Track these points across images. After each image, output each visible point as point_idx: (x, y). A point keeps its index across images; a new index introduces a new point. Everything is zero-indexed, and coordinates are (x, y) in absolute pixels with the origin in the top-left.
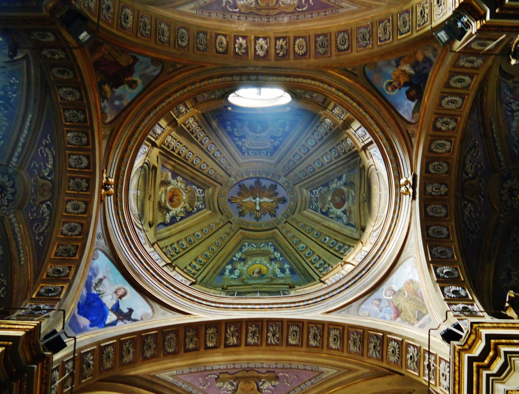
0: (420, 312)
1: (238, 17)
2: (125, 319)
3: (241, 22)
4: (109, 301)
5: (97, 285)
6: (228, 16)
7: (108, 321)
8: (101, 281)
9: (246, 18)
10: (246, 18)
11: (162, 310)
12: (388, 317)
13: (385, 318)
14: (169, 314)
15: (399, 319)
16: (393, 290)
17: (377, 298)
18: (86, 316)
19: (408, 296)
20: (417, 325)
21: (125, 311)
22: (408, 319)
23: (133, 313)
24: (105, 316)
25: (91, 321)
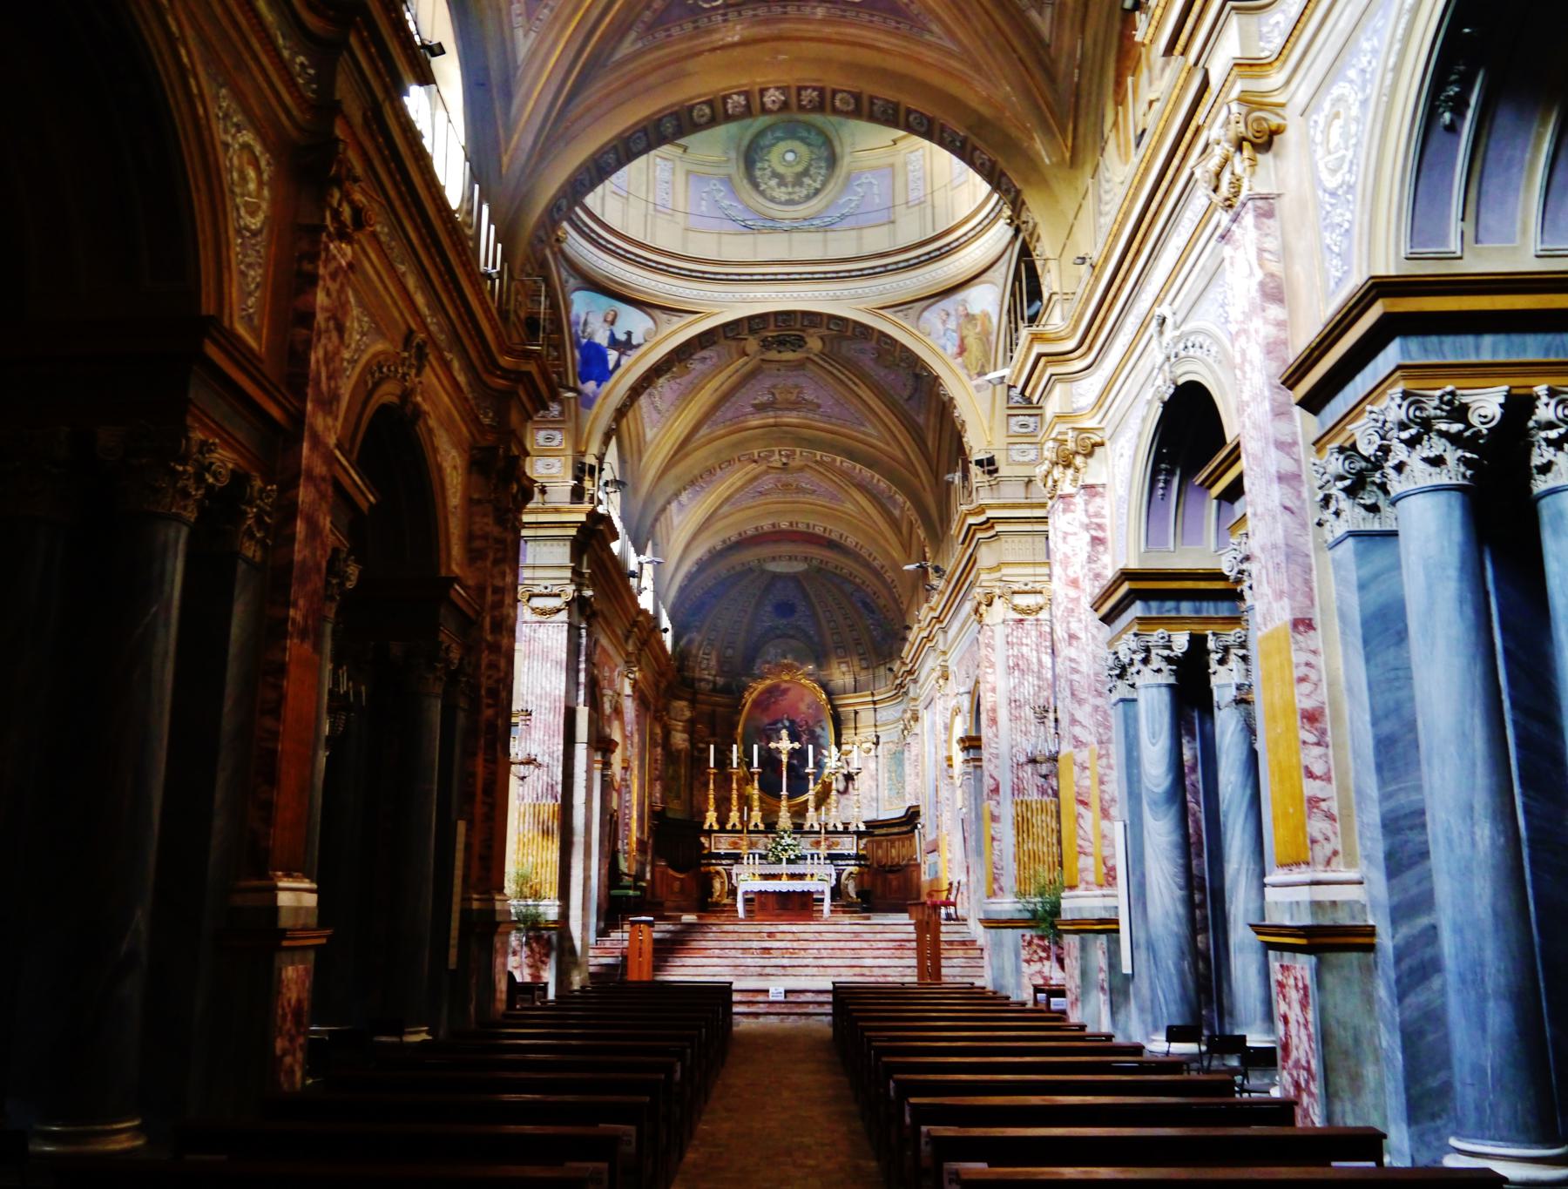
0: (983, 366)
1: (724, 15)
3: (730, 24)
4: (601, 338)
6: (703, 22)
9: (740, 14)
10: (740, 14)
11: (665, 317)
14: (675, 319)
15: (960, 360)
20: (975, 383)
21: (622, 337)
24: (606, 362)
25: (596, 380)
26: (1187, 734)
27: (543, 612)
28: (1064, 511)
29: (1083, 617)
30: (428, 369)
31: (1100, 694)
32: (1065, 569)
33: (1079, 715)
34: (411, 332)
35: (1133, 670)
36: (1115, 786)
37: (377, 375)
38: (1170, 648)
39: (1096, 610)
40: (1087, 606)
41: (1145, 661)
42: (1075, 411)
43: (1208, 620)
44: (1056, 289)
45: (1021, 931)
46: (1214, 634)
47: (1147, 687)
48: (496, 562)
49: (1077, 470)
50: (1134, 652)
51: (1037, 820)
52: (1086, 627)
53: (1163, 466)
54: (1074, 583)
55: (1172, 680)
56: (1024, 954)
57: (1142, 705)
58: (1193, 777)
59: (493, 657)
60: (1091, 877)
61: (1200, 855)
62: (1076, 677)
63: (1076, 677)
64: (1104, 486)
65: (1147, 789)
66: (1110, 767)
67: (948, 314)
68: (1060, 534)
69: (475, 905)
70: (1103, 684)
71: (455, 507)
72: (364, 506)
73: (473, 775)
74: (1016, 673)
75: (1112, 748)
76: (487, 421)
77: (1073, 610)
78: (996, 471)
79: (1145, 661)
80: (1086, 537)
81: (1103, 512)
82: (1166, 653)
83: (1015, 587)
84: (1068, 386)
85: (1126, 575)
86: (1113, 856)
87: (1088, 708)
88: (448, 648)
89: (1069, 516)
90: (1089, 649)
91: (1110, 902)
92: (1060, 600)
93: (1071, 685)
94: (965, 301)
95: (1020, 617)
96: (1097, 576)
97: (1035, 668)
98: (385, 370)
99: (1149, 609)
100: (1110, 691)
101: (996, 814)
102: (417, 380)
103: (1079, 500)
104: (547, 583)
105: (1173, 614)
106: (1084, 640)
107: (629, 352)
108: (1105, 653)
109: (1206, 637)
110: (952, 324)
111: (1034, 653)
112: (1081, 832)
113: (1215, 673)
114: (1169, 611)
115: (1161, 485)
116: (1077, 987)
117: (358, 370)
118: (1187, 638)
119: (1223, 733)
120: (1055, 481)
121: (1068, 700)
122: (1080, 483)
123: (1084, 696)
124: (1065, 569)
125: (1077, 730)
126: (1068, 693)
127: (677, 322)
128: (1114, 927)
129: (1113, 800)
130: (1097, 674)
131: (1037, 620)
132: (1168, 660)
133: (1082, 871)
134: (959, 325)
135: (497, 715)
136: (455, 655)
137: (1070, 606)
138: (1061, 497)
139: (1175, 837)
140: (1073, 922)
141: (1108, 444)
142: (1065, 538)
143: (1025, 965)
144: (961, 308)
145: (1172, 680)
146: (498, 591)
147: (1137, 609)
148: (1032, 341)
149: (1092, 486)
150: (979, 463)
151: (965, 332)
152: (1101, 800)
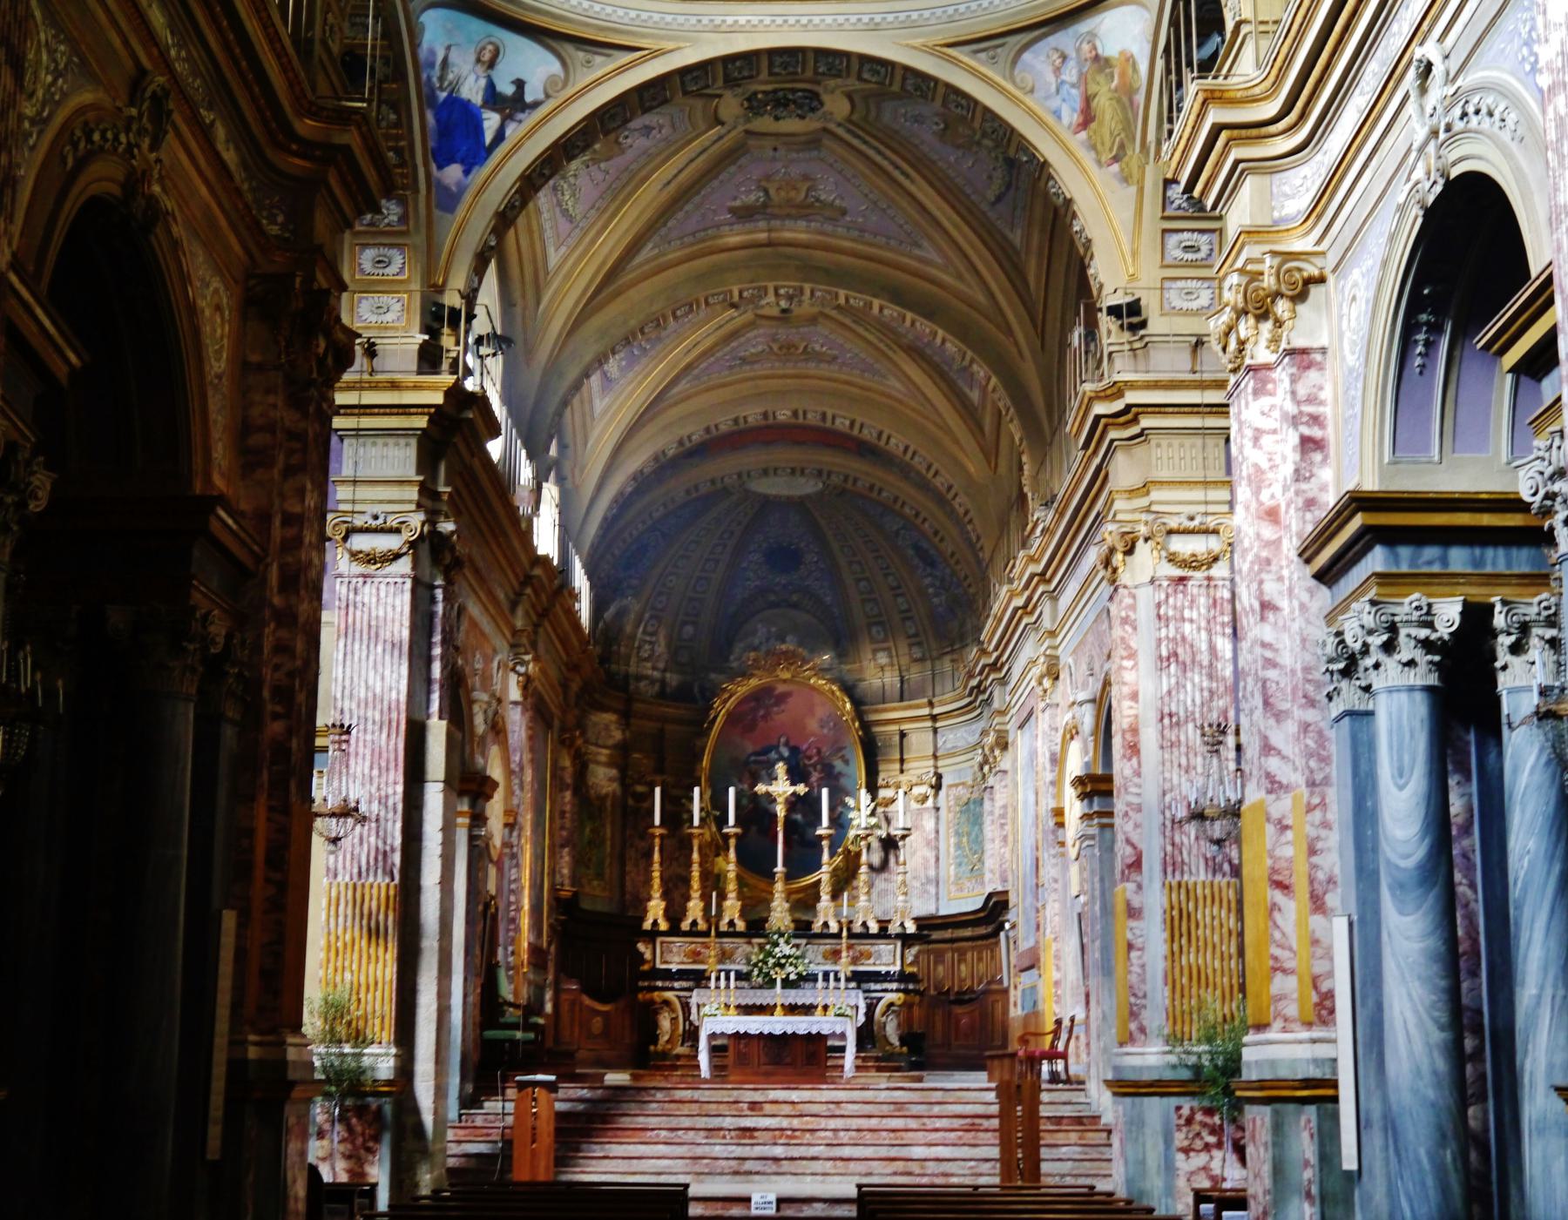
0: (1122, 147)
2: (516, 110)
4: (472, 91)
5: (442, 78)
7: (488, 138)
8: (445, 62)
11: (581, 54)
12: (1066, 120)
13: (1059, 118)
14: (599, 59)
15: (1083, 135)
16: (1095, 48)
17: (1061, 47)
18: (450, 161)
19: (1116, 90)
21: (507, 89)
22: (1099, 147)
23: (527, 89)
25: (462, 162)
26: (1456, 771)
27: (370, 559)
28: (1257, 393)
29: (1285, 573)
30: (170, 136)
31: (1311, 703)
32: (1257, 492)
33: (1277, 739)
34: (142, 72)
35: (1369, 662)
36: (1336, 858)
37: (82, 145)
38: (1430, 625)
39: (1308, 561)
40: (1293, 555)
41: (1389, 647)
42: (1276, 223)
43: (1495, 579)
44: (1247, 14)
45: (1174, 1101)
46: (1504, 603)
47: (1390, 690)
48: (289, 471)
49: (1279, 323)
50: (1371, 632)
51: (1204, 915)
52: (1291, 590)
53: (1424, 317)
54: (1272, 515)
55: (1433, 680)
56: (1180, 1139)
57: (1382, 722)
58: (1466, 843)
59: (283, 633)
60: (1292, 1010)
61: (1474, 973)
62: (1272, 674)
63: (1272, 674)
64: (1323, 350)
65: (1388, 862)
66: (1325, 825)
67: (1064, 57)
68: (1249, 433)
69: (253, 1053)
70: (1318, 685)
71: (219, 377)
72: (62, 372)
73: (250, 833)
74: (1173, 667)
75: (1332, 794)
76: (274, 230)
77: (1268, 562)
78: (1143, 324)
79: (1389, 647)
80: (1293, 438)
81: (1323, 395)
82: (1423, 633)
83: (1173, 523)
84: (1267, 179)
85: (1358, 502)
86: (1330, 974)
87: (1291, 727)
88: (205, 617)
89: (1265, 401)
90: (1296, 626)
91: (1323, 1051)
92: (1246, 544)
93: (1264, 686)
94: (1092, 36)
95: (1179, 572)
96: (1310, 503)
97: (1204, 658)
98: (96, 137)
99: (1397, 560)
100: (1330, 697)
101: (1136, 903)
102: (153, 156)
103: (1282, 375)
104: (378, 509)
105: (1436, 569)
106: (1286, 611)
107: (520, 116)
108: (1321, 632)
109: (1492, 606)
110: (1070, 74)
111: (1204, 635)
112: (1277, 935)
113: (1504, 668)
114: (1430, 563)
115: (1420, 349)
116: (1266, 1192)
117: (49, 135)
118: (1459, 608)
119: (1516, 770)
120: (1242, 343)
121: (1259, 713)
122: (1283, 345)
123: (1285, 706)
124: (1257, 492)
125: (1273, 764)
126: (1258, 701)
127: (603, 64)
128: (1330, 1092)
129: (1331, 881)
130: (1307, 669)
131: (1209, 579)
132: (1427, 645)
133: (1280, 998)
134: (1081, 74)
135: (290, 732)
136: (218, 629)
137: (1264, 554)
138: (1250, 369)
139: (1434, 943)
140: (1262, 1084)
141: (1331, 279)
142: (1256, 440)
143: (1180, 1156)
144: (1086, 47)
145: (1433, 680)
146: (289, 520)
147: (1376, 560)
148: (1204, 102)
149: (1304, 351)
150: (1115, 311)
151: (1092, 88)
152: (1312, 881)
